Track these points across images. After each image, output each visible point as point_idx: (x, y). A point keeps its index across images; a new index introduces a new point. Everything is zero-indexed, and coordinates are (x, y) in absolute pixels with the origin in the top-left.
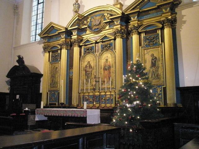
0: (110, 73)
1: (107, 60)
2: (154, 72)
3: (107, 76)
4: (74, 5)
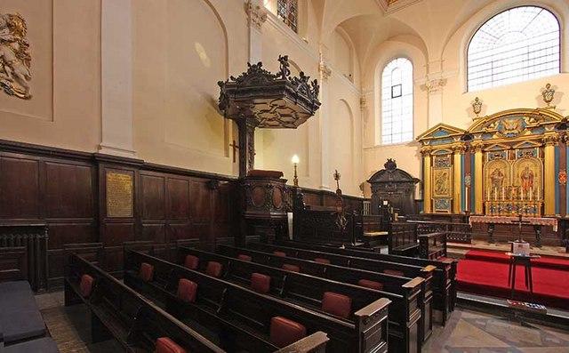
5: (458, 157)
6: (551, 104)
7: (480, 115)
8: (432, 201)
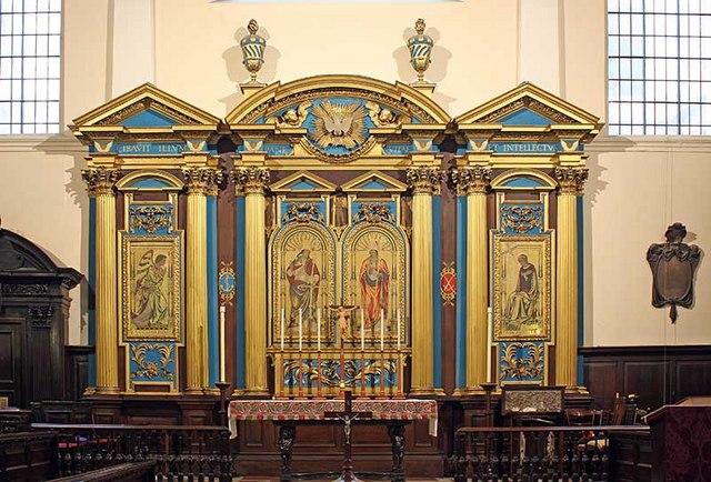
0: (386, 294)
2: (524, 304)
3: (375, 304)
4: (247, 46)
5: (198, 204)
6: (428, 77)
7: (263, 77)
8: (121, 350)
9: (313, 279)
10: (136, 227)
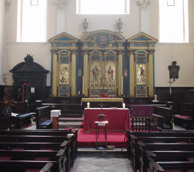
0: (113, 75)
1: (110, 67)
5: (74, 57)
6: (121, 30)
8: (58, 87)
9: (97, 72)
10: (61, 61)
